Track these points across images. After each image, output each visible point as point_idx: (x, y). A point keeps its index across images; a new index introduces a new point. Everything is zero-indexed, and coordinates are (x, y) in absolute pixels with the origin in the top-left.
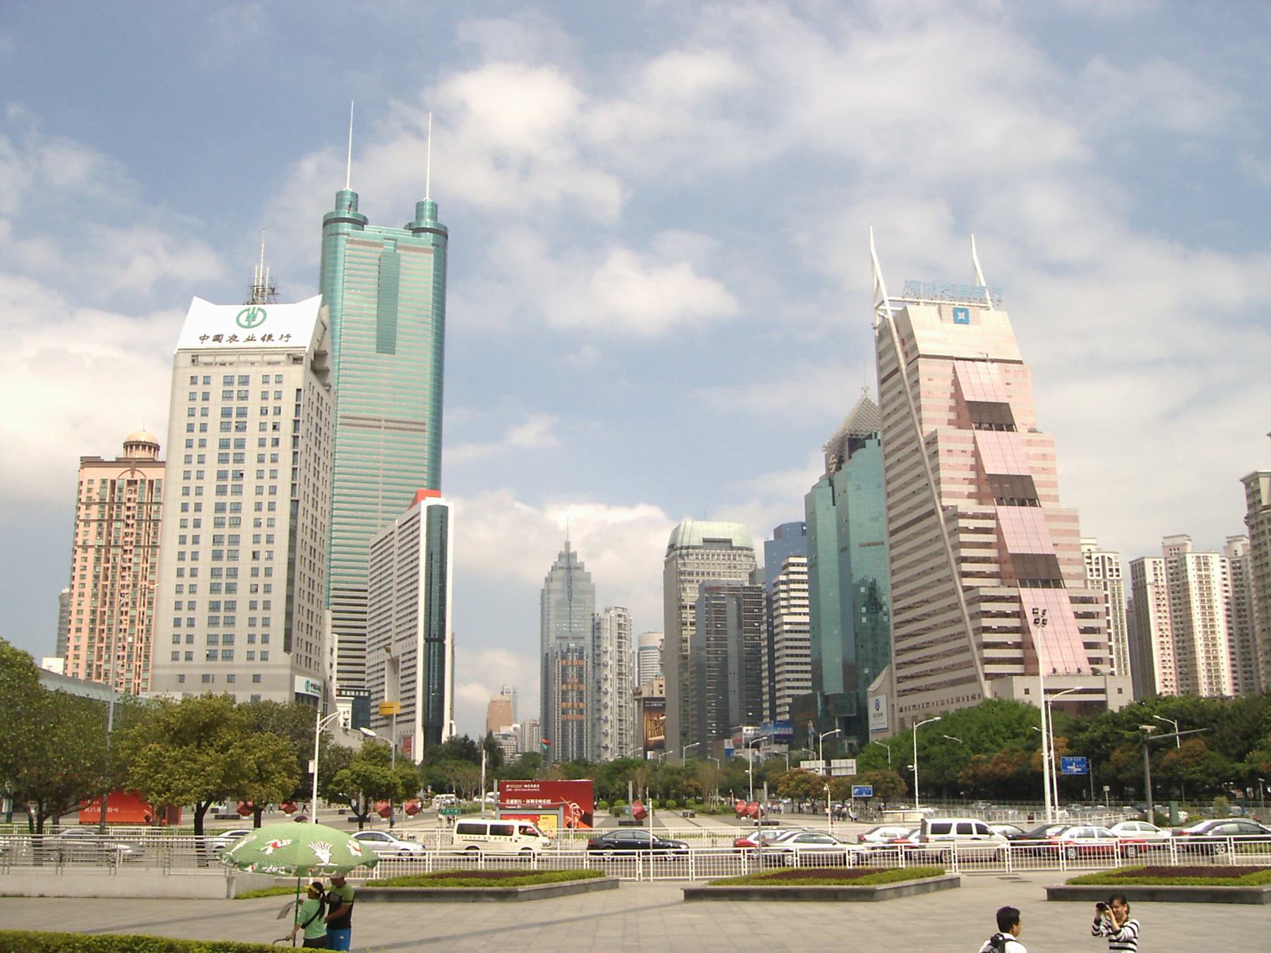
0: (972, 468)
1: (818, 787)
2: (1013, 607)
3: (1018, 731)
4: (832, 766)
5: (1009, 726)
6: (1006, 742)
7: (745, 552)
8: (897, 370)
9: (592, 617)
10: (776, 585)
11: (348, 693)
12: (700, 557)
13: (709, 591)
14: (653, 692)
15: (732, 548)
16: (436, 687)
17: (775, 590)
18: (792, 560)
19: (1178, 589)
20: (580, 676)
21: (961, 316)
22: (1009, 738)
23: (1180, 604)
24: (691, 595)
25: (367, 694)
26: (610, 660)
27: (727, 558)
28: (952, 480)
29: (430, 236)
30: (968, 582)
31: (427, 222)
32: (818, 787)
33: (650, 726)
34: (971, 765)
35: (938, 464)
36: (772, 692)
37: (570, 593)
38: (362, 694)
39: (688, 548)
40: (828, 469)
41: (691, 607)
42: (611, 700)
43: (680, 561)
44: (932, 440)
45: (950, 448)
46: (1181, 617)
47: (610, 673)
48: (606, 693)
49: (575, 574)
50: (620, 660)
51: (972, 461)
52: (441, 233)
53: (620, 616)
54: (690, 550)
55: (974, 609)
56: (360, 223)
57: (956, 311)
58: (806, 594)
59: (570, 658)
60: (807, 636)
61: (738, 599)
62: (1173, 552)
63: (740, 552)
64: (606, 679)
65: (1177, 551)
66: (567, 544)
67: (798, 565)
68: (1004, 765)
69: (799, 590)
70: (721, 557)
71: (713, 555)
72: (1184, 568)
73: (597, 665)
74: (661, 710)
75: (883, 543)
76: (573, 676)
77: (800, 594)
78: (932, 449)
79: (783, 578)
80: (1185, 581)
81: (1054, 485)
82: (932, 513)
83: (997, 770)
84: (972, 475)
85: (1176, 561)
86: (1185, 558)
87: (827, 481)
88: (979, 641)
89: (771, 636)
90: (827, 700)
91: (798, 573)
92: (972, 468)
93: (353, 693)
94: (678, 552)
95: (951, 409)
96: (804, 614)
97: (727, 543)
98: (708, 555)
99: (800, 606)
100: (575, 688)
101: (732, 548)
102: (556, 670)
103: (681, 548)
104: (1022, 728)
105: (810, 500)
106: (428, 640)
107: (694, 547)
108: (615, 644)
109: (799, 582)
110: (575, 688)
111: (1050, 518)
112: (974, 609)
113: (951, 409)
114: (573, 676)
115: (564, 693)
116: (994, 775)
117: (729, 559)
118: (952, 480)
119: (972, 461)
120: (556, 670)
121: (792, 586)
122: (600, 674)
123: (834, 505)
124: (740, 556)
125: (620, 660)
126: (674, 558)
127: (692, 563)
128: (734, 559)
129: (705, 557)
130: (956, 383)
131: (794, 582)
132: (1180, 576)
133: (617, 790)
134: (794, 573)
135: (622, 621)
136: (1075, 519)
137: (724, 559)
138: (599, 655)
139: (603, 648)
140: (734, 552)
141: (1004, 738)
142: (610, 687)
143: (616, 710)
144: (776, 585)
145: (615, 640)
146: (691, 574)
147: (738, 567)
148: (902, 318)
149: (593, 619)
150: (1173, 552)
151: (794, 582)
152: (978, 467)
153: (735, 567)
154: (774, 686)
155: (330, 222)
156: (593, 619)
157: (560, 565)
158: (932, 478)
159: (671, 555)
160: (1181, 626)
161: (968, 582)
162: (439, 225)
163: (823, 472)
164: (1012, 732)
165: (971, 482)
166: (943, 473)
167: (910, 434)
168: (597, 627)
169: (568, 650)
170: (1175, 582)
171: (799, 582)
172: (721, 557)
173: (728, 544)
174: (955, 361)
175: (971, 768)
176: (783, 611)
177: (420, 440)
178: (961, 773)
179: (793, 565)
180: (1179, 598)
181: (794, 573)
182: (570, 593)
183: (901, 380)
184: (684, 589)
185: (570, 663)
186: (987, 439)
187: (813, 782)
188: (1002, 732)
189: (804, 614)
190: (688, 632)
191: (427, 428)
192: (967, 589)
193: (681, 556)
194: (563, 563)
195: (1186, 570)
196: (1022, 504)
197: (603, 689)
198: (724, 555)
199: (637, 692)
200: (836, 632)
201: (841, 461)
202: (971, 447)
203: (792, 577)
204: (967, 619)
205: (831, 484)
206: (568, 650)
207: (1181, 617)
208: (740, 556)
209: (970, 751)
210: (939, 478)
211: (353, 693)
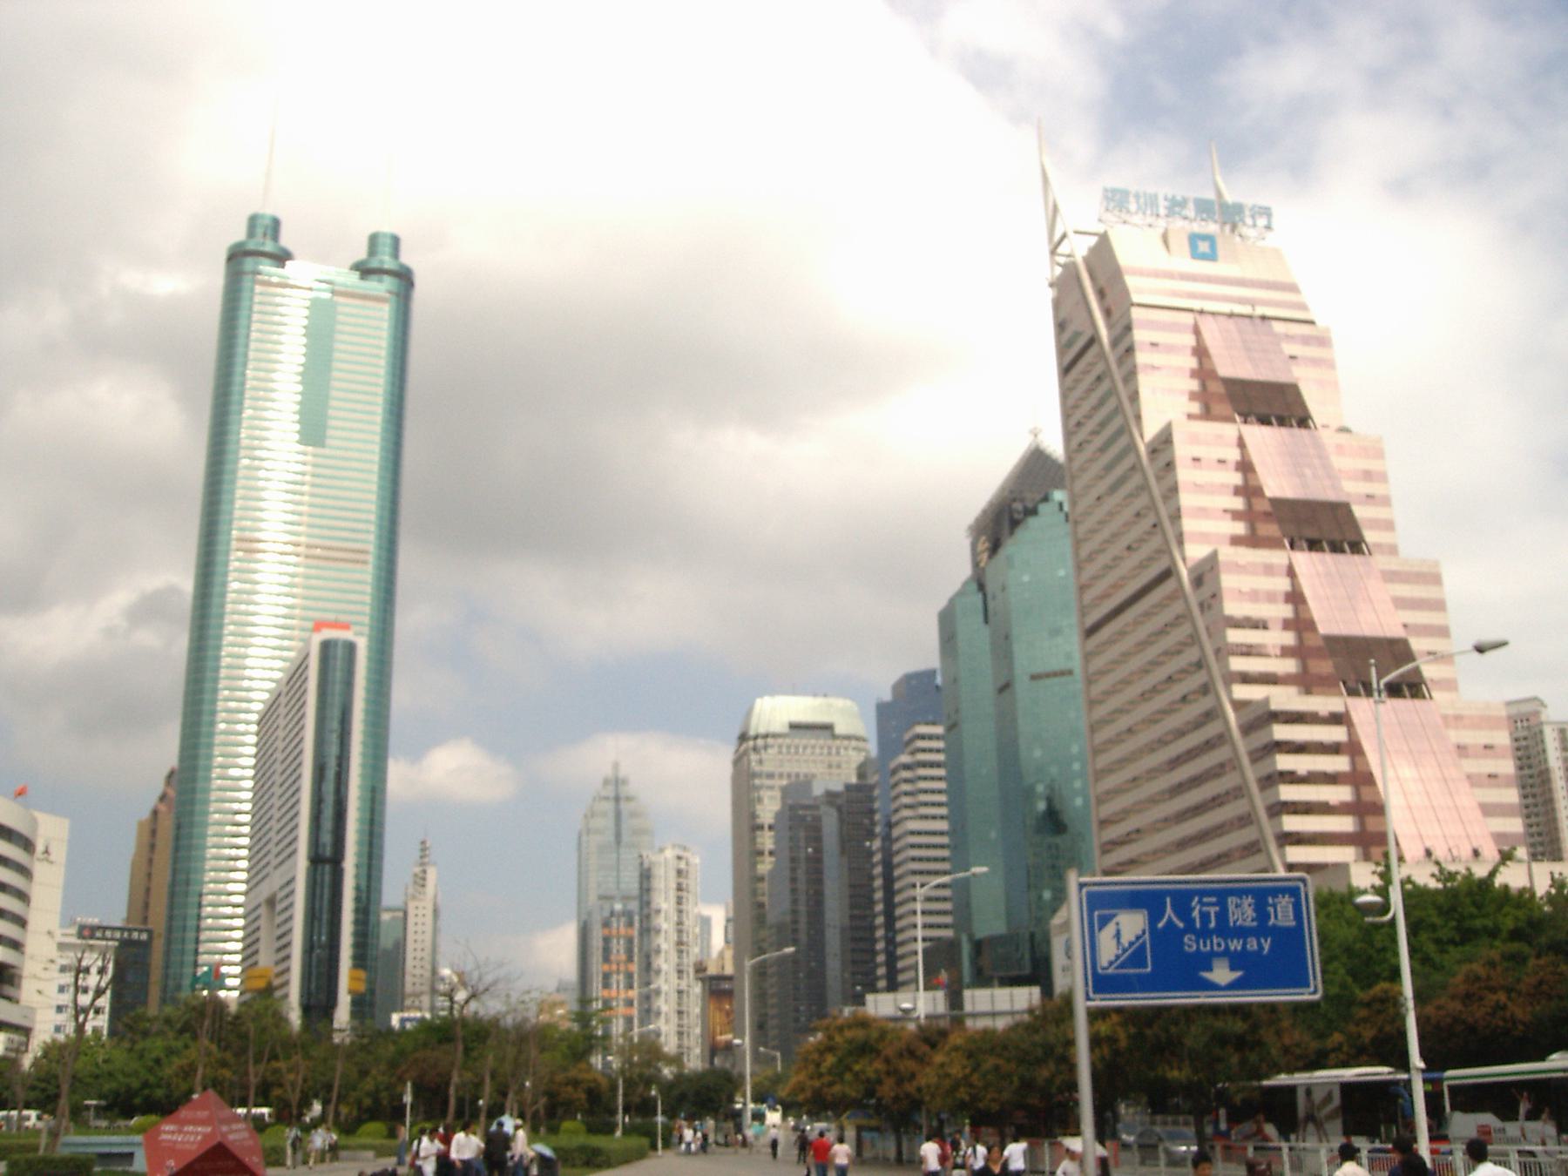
0: (1237, 491)
1: (908, 1065)
2: (1337, 734)
3: (1478, 923)
4: (968, 1007)
5: (1453, 909)
6: (1443, 951)
7: (854, 743)
8: (1093, 340)
9: (639, 861)
10: (894, 772)
11: (108, 934)
12: (784, 750)
13: (795, 792)
14: (723, 968)
15: (834, 737)
16: (324, 938)
17: (894, 793)
18: (922, 729)
19: (1531, 781)
20: (630, 952)
21: (1203, 247)
22: (1452, 942)
23: (1536, 805)
24: (769, 808)
25: (144, 937)
26: (665, 923)
27: (825, 751)
28: (1202, 512)
29: (388, 280)
30: (1242, 692)
31: (388, 263)
32: (908, 1065)
33: (718, 1018)
34: (1363, 1013)
35: (1176, 483)
36: (891, 948)
37: (618, 835)
38: (135, 935)
39: (766, 736)
40: (976, 564)
41: (771, 828)
42: (666, 983)
43: (754, 757)
44: (1165, 440)
45: (1196, 455)
46: (1538, 825)
47: (665, 943)
48: (658, 972)
49: (624, 806)
50: (680, 923)
51: (1237, 479)
52: (405, 277)
53: (679, 858)
54: (770, 741)
55: (1259, 739)
56: (282, 257)
57: (1194, 239)
58: (942, 785)
59: (615, 925)
60: (945, 853)
61: (839, 809)
62: (1519, 724)
63: (846, 743)
64: (658, 951)
65: (1525, 724)
66: (616, 766)
67: (931, 737)
68: (1502, 997)
69: (933, 778)
70: (818, 751)
71: (805, 748)
72: (1540, 748)
73: (647, 930)
74: (729, 994)
75: (1070, 672)
76: (618, 951)
77: (935, 783)
78: (1161, 462)
79: (905, 758)
80: (1543, 767)
81: (1389, 526)
82: (1168, 574)
83: (1478, 1013)
84: (1238, 503)
85: (1525, 739)
86: (1541, 732)
87: (974, 586)
88: (1271, 800)
89: (888, 866)
90: (978, 947)
91: (931, 750)
92: (1237, 491)
93: (118, 935)
94: (751, 743)
95: (1193, 396)
96: (942, 817)
97: (827, 728)
98: (797, 747)
99: (934, 804)
100: (622, 968)
101: (834, 737)
102: (596, 943)
103: (756, 738)
104: (1485, 916)
105: (948, 621)
106: (316, 860)
107: (775, 736)
108: (673, 900)
109: (932, 765)
110: (622, 968)
111: (1391, 577)
112: (1259, 739)
113: (1193, 396)
114: (618, 951)
115: (606, 977)
116: (1472, 1029)
117: (829, 754)
118: (1202, 512)
119: (1237, 479)
120: (596, 943)
121: (922, 772)
122: (650, 943)
123: (986, 620)
124: (846, 749)
125: (680, 923)
126: (745, 753)
127: (770, 761)
128: (838, 753)
129: (793, 750)
130: (1200, 352)
131: (924, 765)
132: (1534, 761)
133: (368, 1094)
134: (924, 750)
135: (682, 865)
136: (1435, 579)
137: (821, 754)
138: (648, 917)
139: (654, 906)
140: (838, 742)
141: (1438, 941)
142: (665, 963)
143: (674, 997)
144: (894, 772)
145: (672, 894)
146: (770, 776)
147: (844, 766)
148: (1102, 251)
149: (642, 864)
150: (1519, 724)
151: (924, 765)
152: (1249, 490)
153: (839, 766)
154: (894, 938)
155: (237, 256)
156: (642, 864)
157: (604, 793)
158: (1164, 513)
159: (742, 748)
160: (1540, 839)
161: (1242, 692)
162: (402, 266)
163: (965, 571)
164: (1458, 929)
165: (1236, 515)
166: (1186, 500)
167: (1123, 442)
168: (646, 876)
169: (612, 914)
170: (1527, 772)
171: (932, 765)
172: (818, 751)
173: (827, 733)
174: (1198, 317)
175: (1365, 1020)
176: (906, 813)
177: (357, 576)
178: (1337, 1037)
179: (922, 737)
180: (1534, 796)
181: (924, 750)
182: (618, 835)
183: (1102, 355)
184: (760, 800)
185: (614, 932)
186: (1263, 440)
187: (889, 1051)
188: (1433, 927)
189: (942, 817)
190: (765, 866)
191: (371, 558)
192: (1239, 705)
193: (755, 749)
194: (610, 792)
195: (1544, 751)
196: (1336, 548)
197: (655, 966)
198: (822, 748)
199: (700, 968)
200: (993, 835)
201: (995, 547)
202: (1234, 455)
203: (922, 757)
204: (1245, 761)
205: (981, 587)
206: (612, 914)
207: (1538, 825)
208: (846, 749)
209: (1349, 980)
210: (1178, 510)
211: (118, 935)
